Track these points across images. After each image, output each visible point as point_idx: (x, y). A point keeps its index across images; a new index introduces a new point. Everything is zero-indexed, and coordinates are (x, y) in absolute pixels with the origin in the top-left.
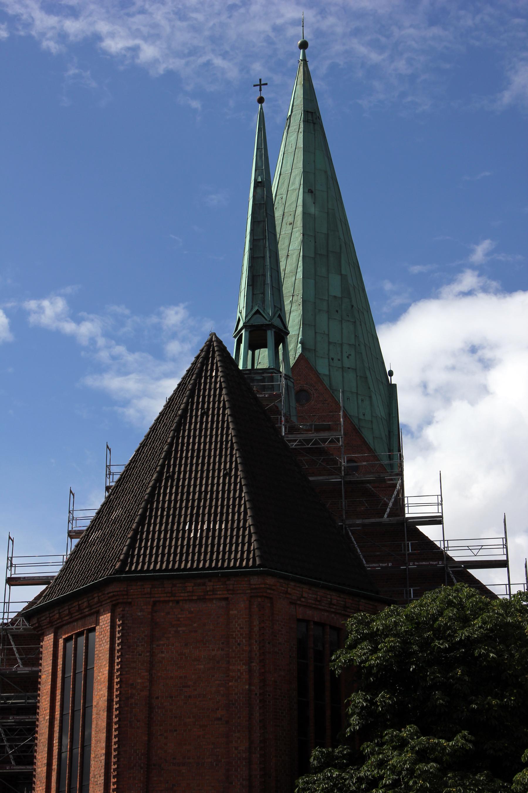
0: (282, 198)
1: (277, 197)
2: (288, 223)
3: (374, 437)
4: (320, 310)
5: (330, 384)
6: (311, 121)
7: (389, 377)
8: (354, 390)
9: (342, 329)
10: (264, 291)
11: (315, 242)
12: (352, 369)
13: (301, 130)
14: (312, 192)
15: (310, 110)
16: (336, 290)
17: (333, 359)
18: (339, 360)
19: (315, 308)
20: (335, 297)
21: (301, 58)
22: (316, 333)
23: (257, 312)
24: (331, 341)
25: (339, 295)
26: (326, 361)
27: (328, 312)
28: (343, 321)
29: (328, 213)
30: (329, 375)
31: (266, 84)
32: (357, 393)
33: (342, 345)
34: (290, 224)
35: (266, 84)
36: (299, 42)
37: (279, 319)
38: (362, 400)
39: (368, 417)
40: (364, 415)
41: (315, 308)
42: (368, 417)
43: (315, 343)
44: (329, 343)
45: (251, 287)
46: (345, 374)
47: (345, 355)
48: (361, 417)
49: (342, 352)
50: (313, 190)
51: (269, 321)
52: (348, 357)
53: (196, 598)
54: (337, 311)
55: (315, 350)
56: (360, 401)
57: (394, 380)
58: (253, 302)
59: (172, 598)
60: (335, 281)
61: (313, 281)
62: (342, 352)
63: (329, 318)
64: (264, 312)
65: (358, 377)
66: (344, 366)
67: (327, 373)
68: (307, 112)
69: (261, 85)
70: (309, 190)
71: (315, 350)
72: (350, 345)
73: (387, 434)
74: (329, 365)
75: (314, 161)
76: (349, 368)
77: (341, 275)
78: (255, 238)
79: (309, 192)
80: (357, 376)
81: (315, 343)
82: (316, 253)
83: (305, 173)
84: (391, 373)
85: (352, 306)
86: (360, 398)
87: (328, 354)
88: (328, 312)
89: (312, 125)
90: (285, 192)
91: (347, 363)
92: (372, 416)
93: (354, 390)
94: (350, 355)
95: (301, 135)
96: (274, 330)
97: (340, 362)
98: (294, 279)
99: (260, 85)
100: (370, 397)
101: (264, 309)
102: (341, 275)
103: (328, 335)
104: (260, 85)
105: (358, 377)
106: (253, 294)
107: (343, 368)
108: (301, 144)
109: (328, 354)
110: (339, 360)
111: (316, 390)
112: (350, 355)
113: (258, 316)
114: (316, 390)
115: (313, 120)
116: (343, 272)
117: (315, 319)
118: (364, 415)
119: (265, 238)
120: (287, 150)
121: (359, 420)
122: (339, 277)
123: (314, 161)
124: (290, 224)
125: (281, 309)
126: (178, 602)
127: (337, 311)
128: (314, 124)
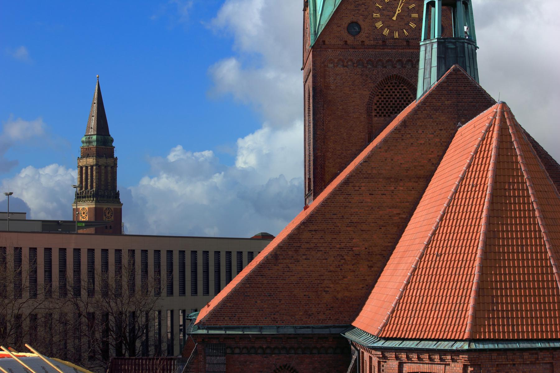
53: (529, 362)
59: (511, 363)
126: (514, 364)
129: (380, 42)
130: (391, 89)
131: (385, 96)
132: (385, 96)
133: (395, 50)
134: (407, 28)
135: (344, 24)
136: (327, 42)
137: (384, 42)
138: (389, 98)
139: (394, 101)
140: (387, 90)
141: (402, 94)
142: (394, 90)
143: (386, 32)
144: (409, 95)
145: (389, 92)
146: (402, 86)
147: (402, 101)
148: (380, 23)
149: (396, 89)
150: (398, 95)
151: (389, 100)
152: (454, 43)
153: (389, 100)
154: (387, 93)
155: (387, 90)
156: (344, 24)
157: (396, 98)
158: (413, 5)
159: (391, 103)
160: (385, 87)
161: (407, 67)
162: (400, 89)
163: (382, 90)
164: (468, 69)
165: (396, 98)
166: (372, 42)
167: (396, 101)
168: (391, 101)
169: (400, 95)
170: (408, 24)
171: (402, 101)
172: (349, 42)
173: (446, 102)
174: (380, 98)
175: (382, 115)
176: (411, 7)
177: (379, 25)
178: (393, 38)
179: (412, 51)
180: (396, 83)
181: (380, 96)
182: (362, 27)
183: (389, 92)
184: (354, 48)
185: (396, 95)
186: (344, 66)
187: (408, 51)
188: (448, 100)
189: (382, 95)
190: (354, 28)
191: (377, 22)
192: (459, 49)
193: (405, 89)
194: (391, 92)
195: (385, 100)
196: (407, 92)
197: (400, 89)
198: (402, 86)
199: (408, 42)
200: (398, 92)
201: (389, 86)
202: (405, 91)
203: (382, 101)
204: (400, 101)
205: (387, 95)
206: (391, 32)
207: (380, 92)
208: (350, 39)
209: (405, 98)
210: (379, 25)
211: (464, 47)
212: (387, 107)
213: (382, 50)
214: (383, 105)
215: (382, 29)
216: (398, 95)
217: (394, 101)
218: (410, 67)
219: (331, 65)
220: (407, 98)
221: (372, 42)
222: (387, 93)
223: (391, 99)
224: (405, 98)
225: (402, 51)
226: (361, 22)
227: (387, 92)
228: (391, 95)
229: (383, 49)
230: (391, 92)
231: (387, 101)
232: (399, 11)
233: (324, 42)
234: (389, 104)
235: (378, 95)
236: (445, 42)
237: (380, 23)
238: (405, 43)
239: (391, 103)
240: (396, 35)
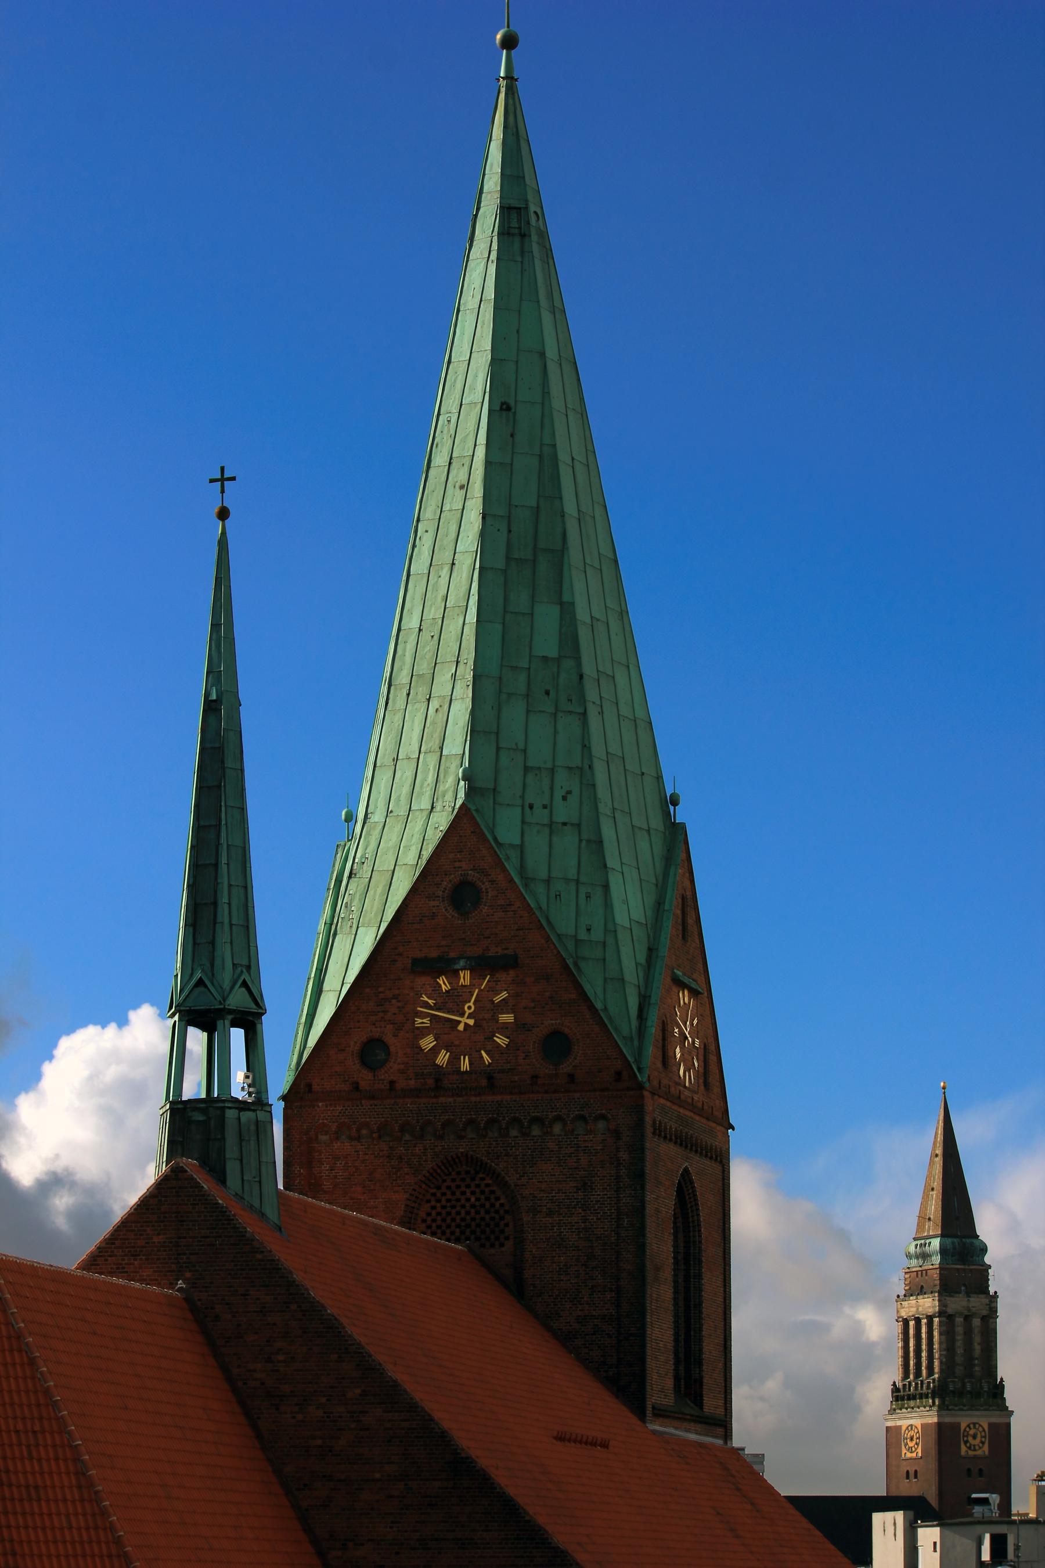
0: (449, 421)
1: (441, 418)
3: (605, 980)
4: (510, 695)
5: (522, 866)
6: (516, 231)
7: (671, 808)
8: (572, 873)
9: (556, 732)
10: (214, 937)
11: (510, 531)
12: (572, 825)
13: (494, 256)
15: (515, 203)
16: (547, 645)
17: (531, 807)
18: (545, 807)
19: (500, 691)
20: (545, 659)
21: (502, 74)
22: (498, 749)
23: (200, 983)
24: (529, 764)
25: (553, 653)
26: (518, 811)
28: (560, 714)
29: (541, 456)
30: (522, 847)
32: (577, 881)
33: (552, 771)
34: (462, 487)
36: (499, 37)
37: (244, 989)
38: (588, 896)
39: (597, 935)
40: (589, 930)
41: (500, 691)
42: (597, 935)
43: (497, 772)
44: (527, 769)
45: (191, 929)
46: (555, 839)
47: (558, 794)
48: (583, 935)
49: (552, 788)
50: (512, 404)
51: (220, 1003)
52: (564, 798)
55: (494, 789)
57: (681, 814)
58: (193, 961)
60: (547, 617)
61: (499, 627)
62: (552, 788)
63: (528, 712)
64: (213, 984)
65: (584, 844)
66: (555, 819)
67: (517, 841)
68: (510, 208)
69: (223, 480)
70: (503, 404)
71: (494, 789)
72: (570, 768)
73: (642, 958)
74: (523, 822)
75: (518, 332)
76: (565, 824)
77: (561, 604)
78: (202, 823)
79: (501, 409)
80: (580, 841)
81: (497, 772)
82: (508, 558)
83: (496, 363)
84: (675, 802)
85: (581, 677)
86: (583, 890)
87: (522, 797)
89: (517, 241)
90: (455, 410)
91: (563, 812)
92: (606, 930)
93: (572, 873)
94: (569, 792)
95: (492, 269)
96: (230, 1017)
97: (546, 811)
98: (461, 622)
99: (222, 480)
100: (606, 887)
101: (213, 975)
103: (525, 751)
104: (222, 480)
105: (584, 844)
106: (195, 944)
107: (551, 825)
108: (490, 293)
109: (522, 797)
110: (545, 807)
111: (492, 882)
112: (569, 792)
113: (202, 989)
114: (492, 882)
115: (520, 228)
116: (566, 598)
117: (499, 718)
118: (589, 930)
119: (220, 824)
120: (465, 304)
121: (578, 942)
122: (556, 610)
123: (518, 332)
124: (462, 487)
125: (248, 968)
127: (547, 693)
128: (523, 236)
129: (431, 1082)
130: (458, 1187)
131: (444, 1203)
132: (444, 1203)
133: (460, 1099)
134: (489, 1047)
135: (352, 1043)
136: (315, 1087)
137: (439, 1081)
138: (453, 1207)
139: (463, 1212)
140: (449, 1187)
141: (483, 1197)
142: (463, 1189)
143: (443, 1058)
144: (497, 1199)
145: (453, 1194)
146: (482, 1179)
147: (482, 1211)
148: (431, 1038)
149: (468, 1186)
150: (473, 1199)
151: (454, 1211)
152: (204, 1111)
153: (454, 1211)
154: (449, 1196)
155: (449, 1187)
156: (352, 1043)
157: (468, 1205)
158: (504, 995)
159: (458, 1218)
160: (444, 1181)
161: (490, 1134)
162: (478, 1186)
163: (439, 1188)
164: (232, 1168)
165: (468, 1205)
166: (412, 1082)
167: (468, 1213)
168: (458, 1213)
169: (478, 1199)
170: (490, 1038)
171: (482, 1211)
172: (362, 1084)
173: (155, 1239)
174: (433, 1208)
175: (497, 1243)
176: (498, 999)
177: (428, 1043)
178: (458, 1071)
179: (499, 1098)
180: (467, 1172)
181: (433, 1203)
182: (392, 1049)
183: (453, 1194)
184: (373, 1098)
185: (468, 1200)
186: (351, 1139)
187: (490, 1098)
188: (159, 1234)
189: (439, 1201)
190: (372, 1053)
191: (424, 1036)
192: (212, 1123)
193: (487, 1185)
194: (458, 1193)
195: (444, 1212)
196: (492, 1192)
197: (478, 1186)
198: (482, 1179)
199: (490, 1078)
200: (473, 1193)
201: (453, 1180)
202: (487, 1190)
203: (439, 1214)
204: (478, 1212)
205: (449, 1201)
206: (454, 1060)
207: (434, 1194)
208: (365, 1078)
209: (488, 1205)
210: (428, 1043)
211: (222, 1118)
212: (449, 1226)
213: (434, 1100)
214: (439, 1222)
215: (435, 1051)
216: (473, 1199)
217: (463, 1212)
218: (496, 1135)
219: (324, 1138)
220: (493, 1205)
221: (412, 1082)
222: (449, 1196)
223: (458, 1209)
224: (488, 1205)
225: (478, 1099)
226: (390, 1040)
227: (449, 1193)
228: (458, 1200)
229: (436, 1097)
230: (458, 1193)
231: (449, 1213)
232: (469, 1008)
233: (309, 1086)
234: (453, 1220)
235: (428, 1201)
236: (185, 1109)
237: (431, 1038)
238: (484, 1082)
239: (458, 1218)
240: (465, 1064)
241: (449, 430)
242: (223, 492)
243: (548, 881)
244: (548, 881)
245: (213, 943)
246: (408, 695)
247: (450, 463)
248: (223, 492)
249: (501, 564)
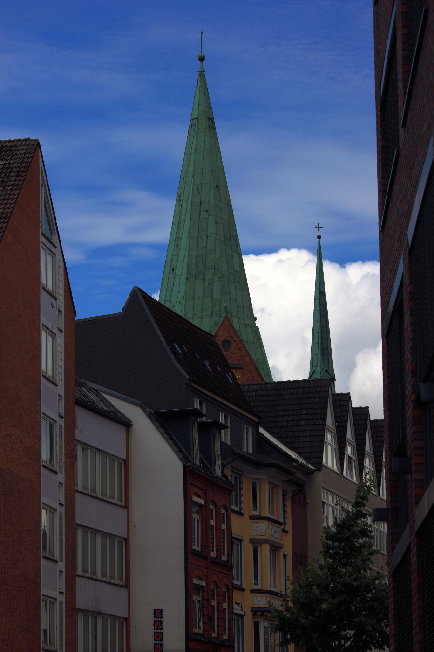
0: (198, 188)
2: (205, 210)
14: (218, 187)
22: (230, 299)
23: (326, 371)
27: (235, 283)
31: (319, 224)
34: (207, 211)
35: (319, 224)
44: (238, 306)
47: (245, 315)
48: (258, 360)
52: (247, 316)
54: (239, 282)
56: (256, 349)
67: (239, 329)
74: (239, 323)
77: (238, 254)
88: (235, 283)
89: (213, 129)
94: (248, 315)
102: (238, 254)
107: (245, 324)
109: (238, 315)
114: (234, 341)
116: (239, 252)
121: (257, 362)
127: (239, 282)
241: (198, 191)
242: (319, 231)
243: (247, 342)
244: (247, 342)
245: (328, 360)
246: (195, 277)
247: (201, 203)
248: (319, 231)
249: (223, 239)
